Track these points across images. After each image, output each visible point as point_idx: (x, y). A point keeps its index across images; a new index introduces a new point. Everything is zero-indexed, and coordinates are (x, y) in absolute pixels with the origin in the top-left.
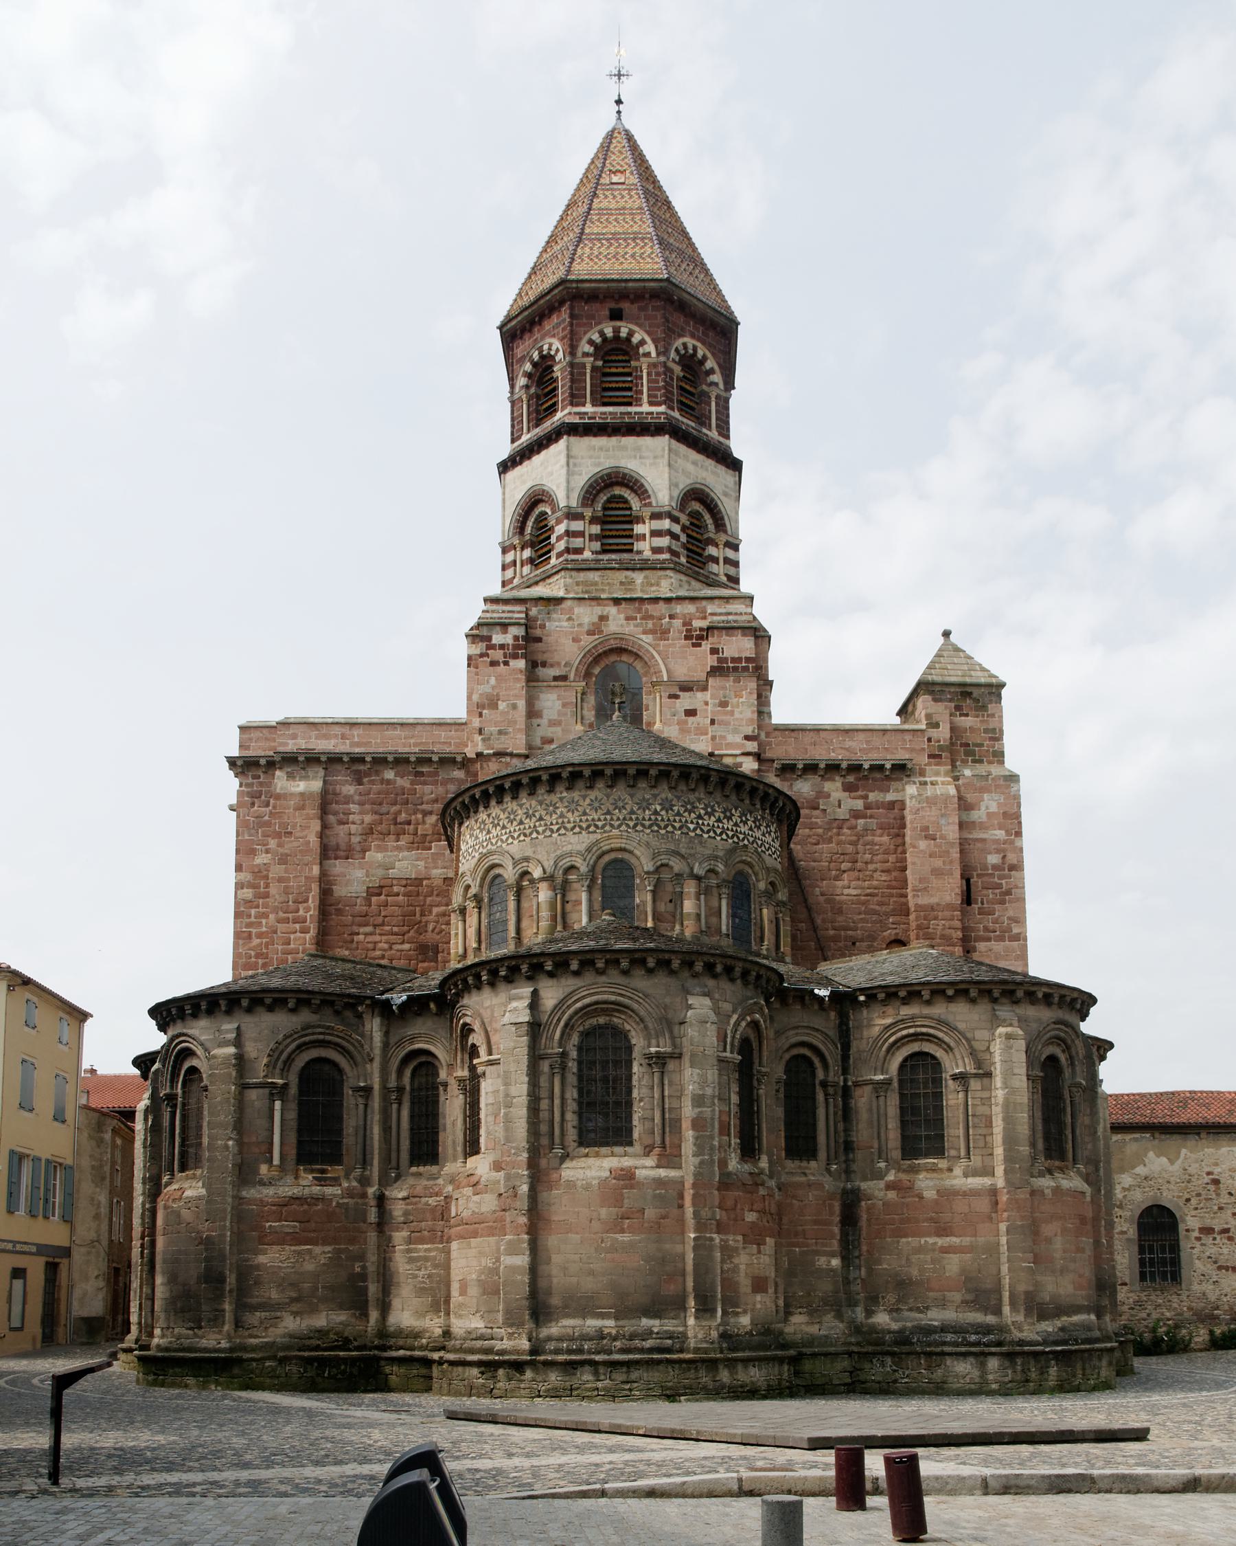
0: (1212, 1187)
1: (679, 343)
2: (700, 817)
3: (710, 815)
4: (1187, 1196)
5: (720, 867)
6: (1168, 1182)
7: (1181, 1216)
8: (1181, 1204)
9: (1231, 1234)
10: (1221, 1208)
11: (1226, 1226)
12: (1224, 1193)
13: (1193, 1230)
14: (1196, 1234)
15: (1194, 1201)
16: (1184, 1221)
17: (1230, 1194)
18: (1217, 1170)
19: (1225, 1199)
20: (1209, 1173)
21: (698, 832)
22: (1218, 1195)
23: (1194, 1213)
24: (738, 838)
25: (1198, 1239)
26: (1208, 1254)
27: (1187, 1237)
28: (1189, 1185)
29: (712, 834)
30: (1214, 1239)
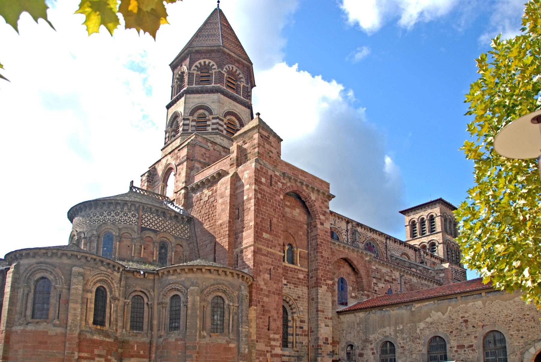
0: (464, 324)
1: (197, 63)
2: (91, 218)
3: (94, 216)
4: (451, 330)
5: (95, 233)
6: (442, 324)
7: (448, 341)
8: (448, 334)
9: (474, 348)
10: (468, 335)
11: (471, 344)
12: (470, 326)
13: (454, 347)
14: (455, 349)
15: (454, 332)
16: (449, 343)
17: (474, 327)
18: (466, 315)
19: (471, 329)
20: (462, 317)
21: (90, 223)
22: (467, 328)
23: (454, 338)
24: (105, 221)
25: (456, 351)
26: (461, 359)
27: (451, 351)
28: (452, 325)
29: (94, 222)
30: (465, 351)
